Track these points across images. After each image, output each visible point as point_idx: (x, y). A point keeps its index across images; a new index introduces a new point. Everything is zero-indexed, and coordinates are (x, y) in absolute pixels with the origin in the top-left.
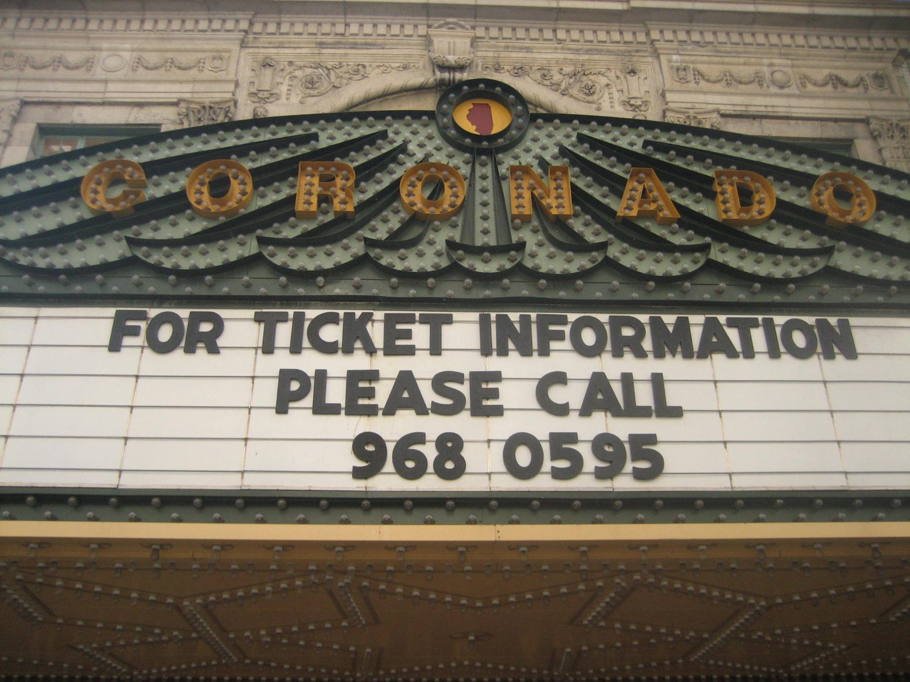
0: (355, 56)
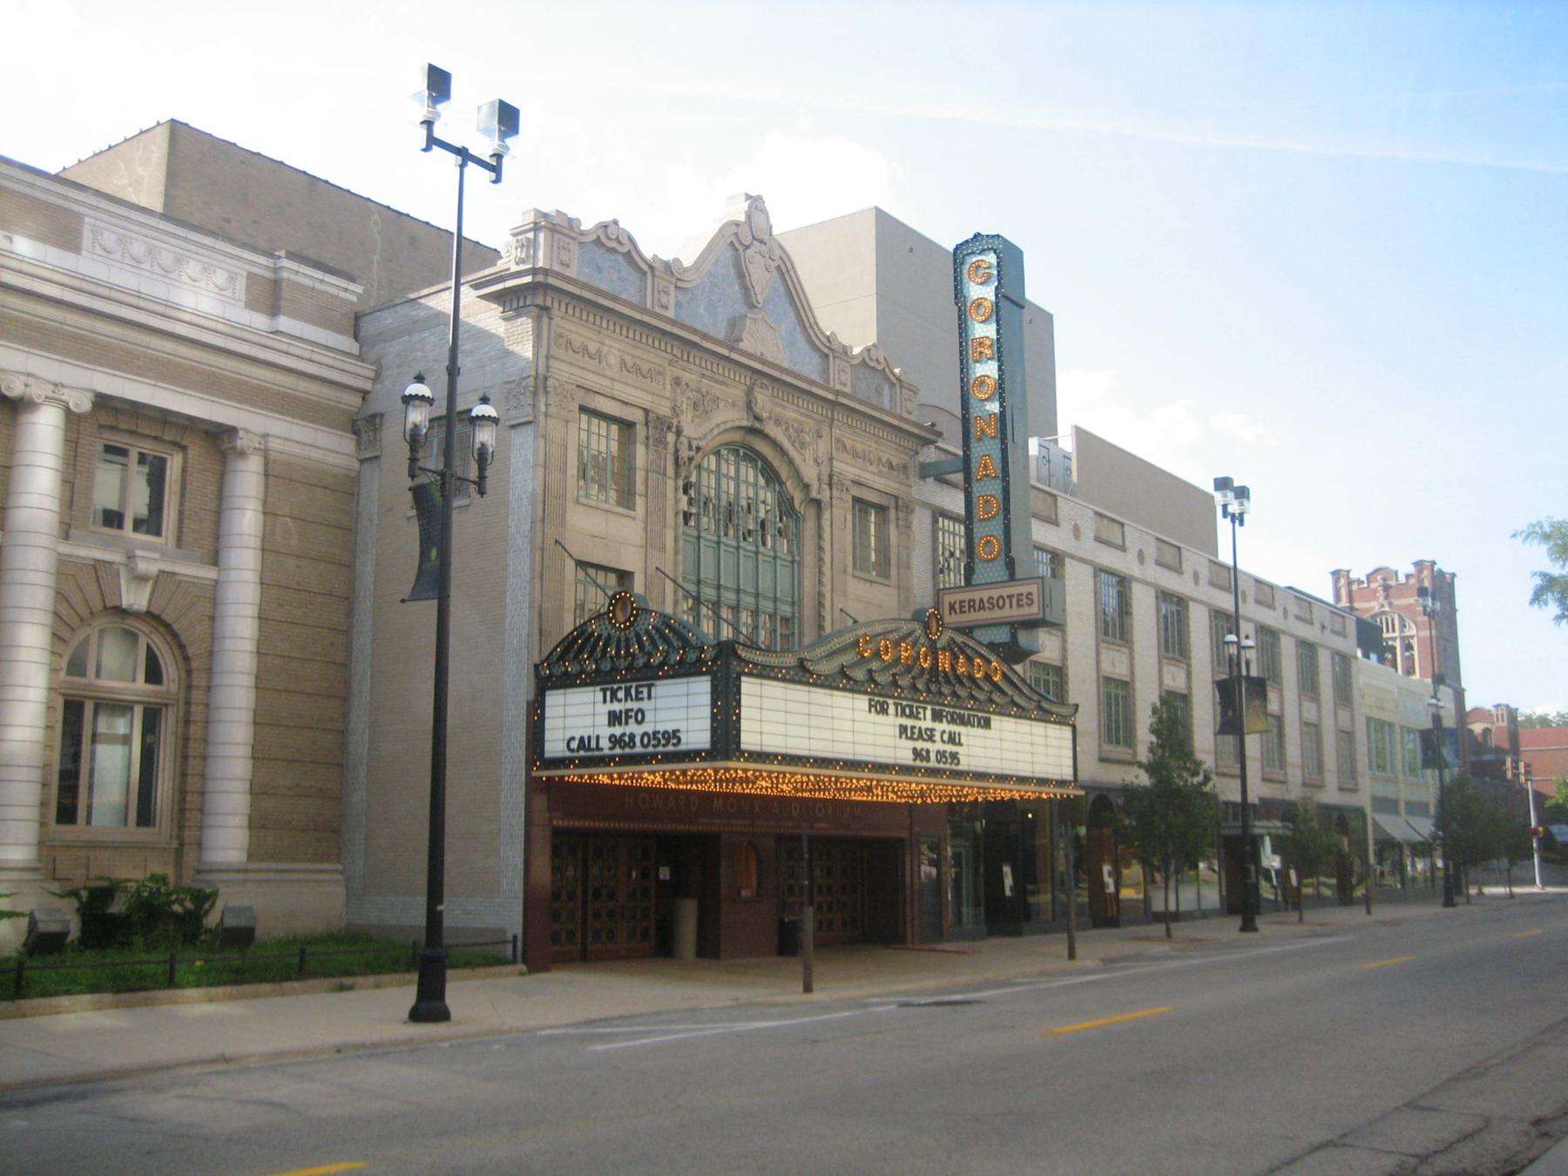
0: (717, 390)
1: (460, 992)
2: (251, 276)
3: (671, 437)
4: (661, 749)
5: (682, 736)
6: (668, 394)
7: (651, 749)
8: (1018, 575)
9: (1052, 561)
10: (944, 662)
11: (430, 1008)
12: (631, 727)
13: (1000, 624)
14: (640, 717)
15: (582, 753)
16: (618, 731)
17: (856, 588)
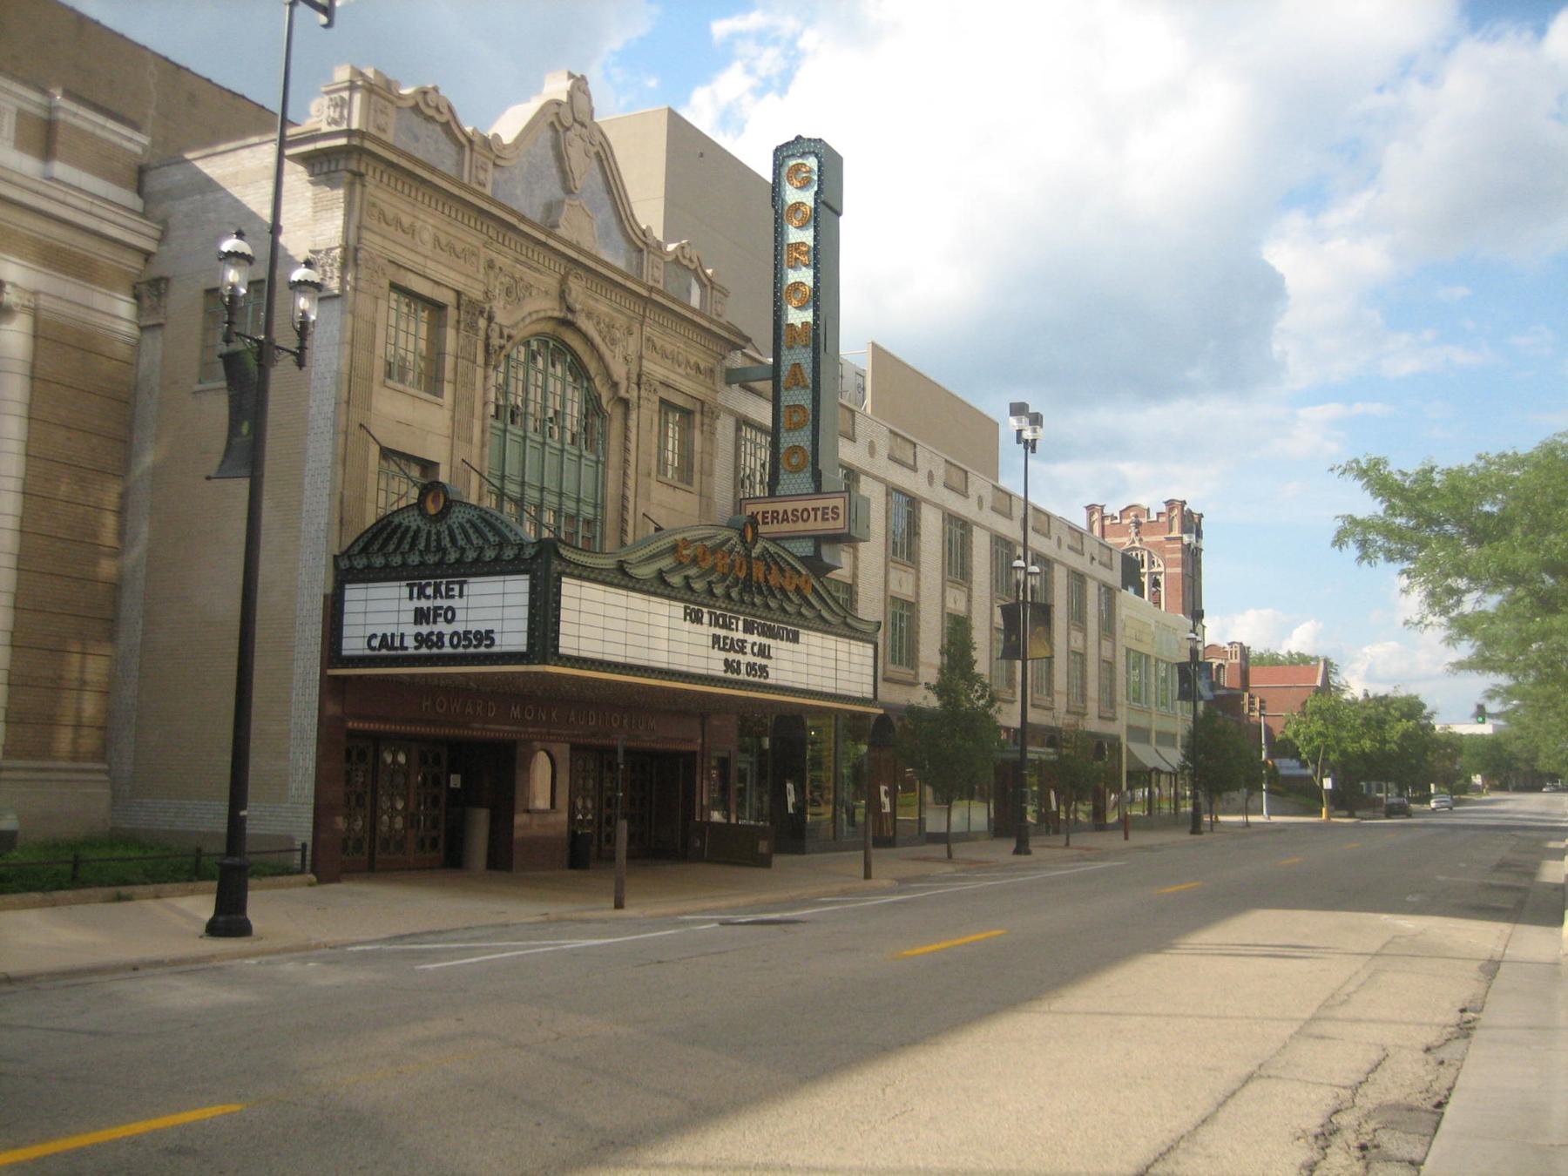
0: (530, 276)
1: (266, 906)
2: (21, 114)
3: (482, 323)
4: (471, 650)
5: (496, 637)
6: (481, 277)
7: (461, 650)
8: (824, 489)
9: (846, 476)
10: (759, 572)
11: (229, 921)
12: (441, 626)
13: (804, 537)
14: (450, 615)
15: (384, 652)
16: (424, 629)
17: (660, 493)
